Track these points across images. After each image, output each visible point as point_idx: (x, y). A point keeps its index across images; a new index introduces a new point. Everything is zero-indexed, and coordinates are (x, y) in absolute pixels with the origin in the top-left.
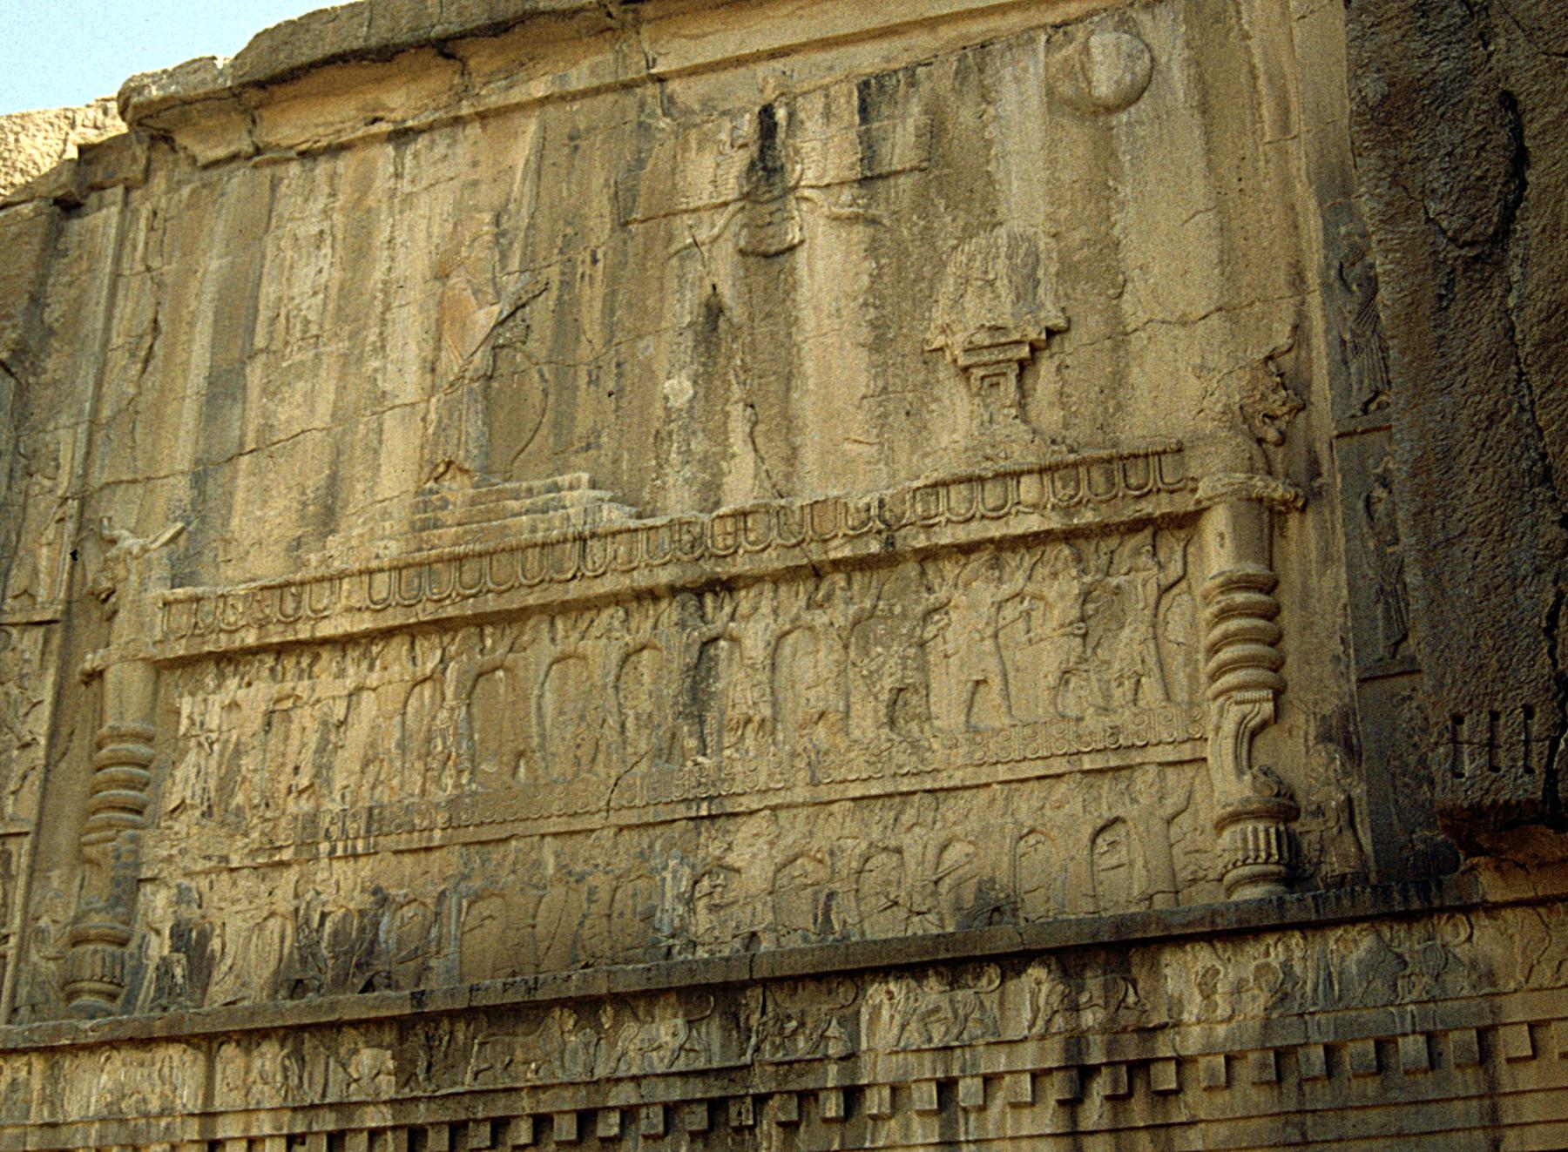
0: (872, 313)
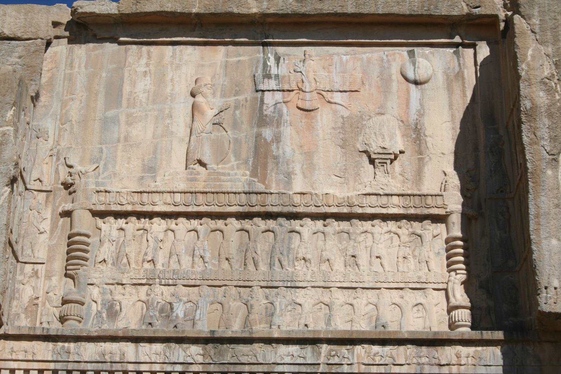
0: (341, 136)
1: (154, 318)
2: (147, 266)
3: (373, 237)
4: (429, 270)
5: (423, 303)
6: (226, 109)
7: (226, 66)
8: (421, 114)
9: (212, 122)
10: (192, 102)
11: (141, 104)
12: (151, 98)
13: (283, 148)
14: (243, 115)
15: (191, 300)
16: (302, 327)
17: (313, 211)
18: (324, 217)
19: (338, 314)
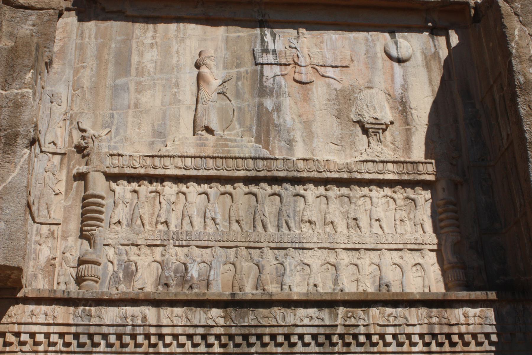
0: (336, 107)
1: (170, 278)
2: (160, 227)
3: (371, 200)
4: (424, 232)
5: (421, 263)
6: (229, 80)
8: (405, 88)
9: (217, 92)
11: (149, 74)
12: (158, 68)
13: (283, 117)
14: (245, 86)
15: (204, 260)
16: (311, 288)
17: (316, 176)
18: (325, 182)
19: (344, 274)
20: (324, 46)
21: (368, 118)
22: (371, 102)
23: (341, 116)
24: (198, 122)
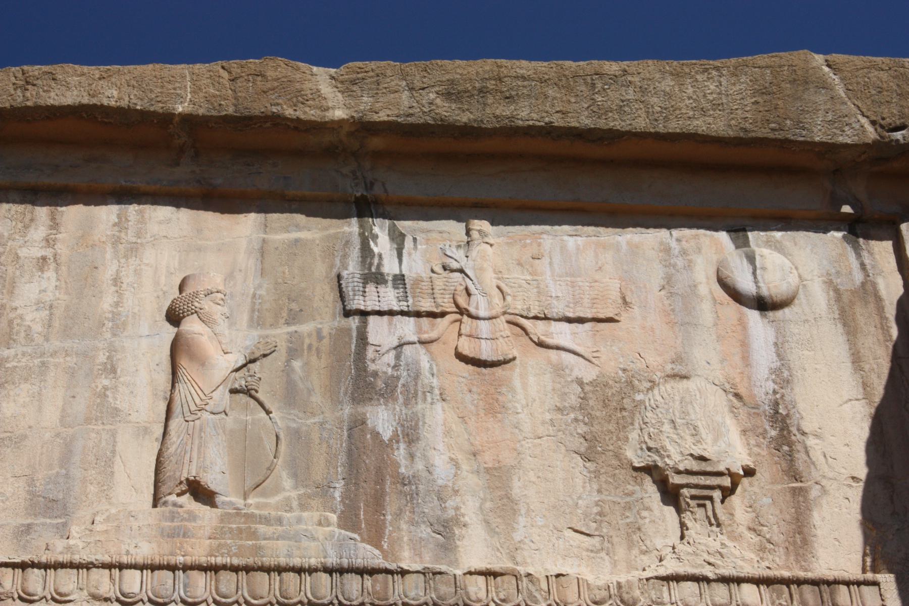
0: (582, 429)
6: (265, 356)
7: (263, 251)
9: (229, 387)
10: (172, 336)
12: (56, 324)
20: (543, 265)
21: (677, 457)
22: (685, 413)
23: (597, 453)
24: (169, 468)
